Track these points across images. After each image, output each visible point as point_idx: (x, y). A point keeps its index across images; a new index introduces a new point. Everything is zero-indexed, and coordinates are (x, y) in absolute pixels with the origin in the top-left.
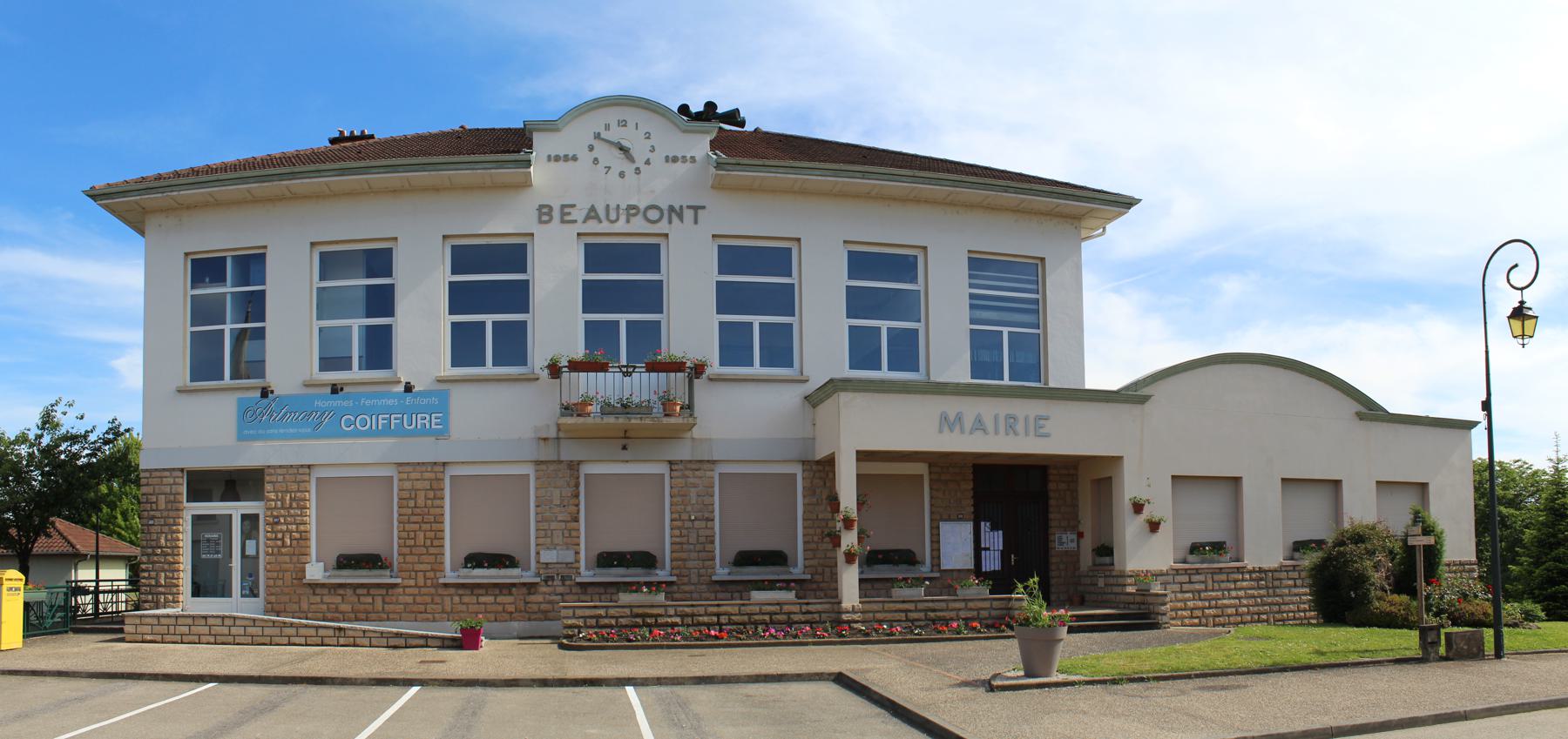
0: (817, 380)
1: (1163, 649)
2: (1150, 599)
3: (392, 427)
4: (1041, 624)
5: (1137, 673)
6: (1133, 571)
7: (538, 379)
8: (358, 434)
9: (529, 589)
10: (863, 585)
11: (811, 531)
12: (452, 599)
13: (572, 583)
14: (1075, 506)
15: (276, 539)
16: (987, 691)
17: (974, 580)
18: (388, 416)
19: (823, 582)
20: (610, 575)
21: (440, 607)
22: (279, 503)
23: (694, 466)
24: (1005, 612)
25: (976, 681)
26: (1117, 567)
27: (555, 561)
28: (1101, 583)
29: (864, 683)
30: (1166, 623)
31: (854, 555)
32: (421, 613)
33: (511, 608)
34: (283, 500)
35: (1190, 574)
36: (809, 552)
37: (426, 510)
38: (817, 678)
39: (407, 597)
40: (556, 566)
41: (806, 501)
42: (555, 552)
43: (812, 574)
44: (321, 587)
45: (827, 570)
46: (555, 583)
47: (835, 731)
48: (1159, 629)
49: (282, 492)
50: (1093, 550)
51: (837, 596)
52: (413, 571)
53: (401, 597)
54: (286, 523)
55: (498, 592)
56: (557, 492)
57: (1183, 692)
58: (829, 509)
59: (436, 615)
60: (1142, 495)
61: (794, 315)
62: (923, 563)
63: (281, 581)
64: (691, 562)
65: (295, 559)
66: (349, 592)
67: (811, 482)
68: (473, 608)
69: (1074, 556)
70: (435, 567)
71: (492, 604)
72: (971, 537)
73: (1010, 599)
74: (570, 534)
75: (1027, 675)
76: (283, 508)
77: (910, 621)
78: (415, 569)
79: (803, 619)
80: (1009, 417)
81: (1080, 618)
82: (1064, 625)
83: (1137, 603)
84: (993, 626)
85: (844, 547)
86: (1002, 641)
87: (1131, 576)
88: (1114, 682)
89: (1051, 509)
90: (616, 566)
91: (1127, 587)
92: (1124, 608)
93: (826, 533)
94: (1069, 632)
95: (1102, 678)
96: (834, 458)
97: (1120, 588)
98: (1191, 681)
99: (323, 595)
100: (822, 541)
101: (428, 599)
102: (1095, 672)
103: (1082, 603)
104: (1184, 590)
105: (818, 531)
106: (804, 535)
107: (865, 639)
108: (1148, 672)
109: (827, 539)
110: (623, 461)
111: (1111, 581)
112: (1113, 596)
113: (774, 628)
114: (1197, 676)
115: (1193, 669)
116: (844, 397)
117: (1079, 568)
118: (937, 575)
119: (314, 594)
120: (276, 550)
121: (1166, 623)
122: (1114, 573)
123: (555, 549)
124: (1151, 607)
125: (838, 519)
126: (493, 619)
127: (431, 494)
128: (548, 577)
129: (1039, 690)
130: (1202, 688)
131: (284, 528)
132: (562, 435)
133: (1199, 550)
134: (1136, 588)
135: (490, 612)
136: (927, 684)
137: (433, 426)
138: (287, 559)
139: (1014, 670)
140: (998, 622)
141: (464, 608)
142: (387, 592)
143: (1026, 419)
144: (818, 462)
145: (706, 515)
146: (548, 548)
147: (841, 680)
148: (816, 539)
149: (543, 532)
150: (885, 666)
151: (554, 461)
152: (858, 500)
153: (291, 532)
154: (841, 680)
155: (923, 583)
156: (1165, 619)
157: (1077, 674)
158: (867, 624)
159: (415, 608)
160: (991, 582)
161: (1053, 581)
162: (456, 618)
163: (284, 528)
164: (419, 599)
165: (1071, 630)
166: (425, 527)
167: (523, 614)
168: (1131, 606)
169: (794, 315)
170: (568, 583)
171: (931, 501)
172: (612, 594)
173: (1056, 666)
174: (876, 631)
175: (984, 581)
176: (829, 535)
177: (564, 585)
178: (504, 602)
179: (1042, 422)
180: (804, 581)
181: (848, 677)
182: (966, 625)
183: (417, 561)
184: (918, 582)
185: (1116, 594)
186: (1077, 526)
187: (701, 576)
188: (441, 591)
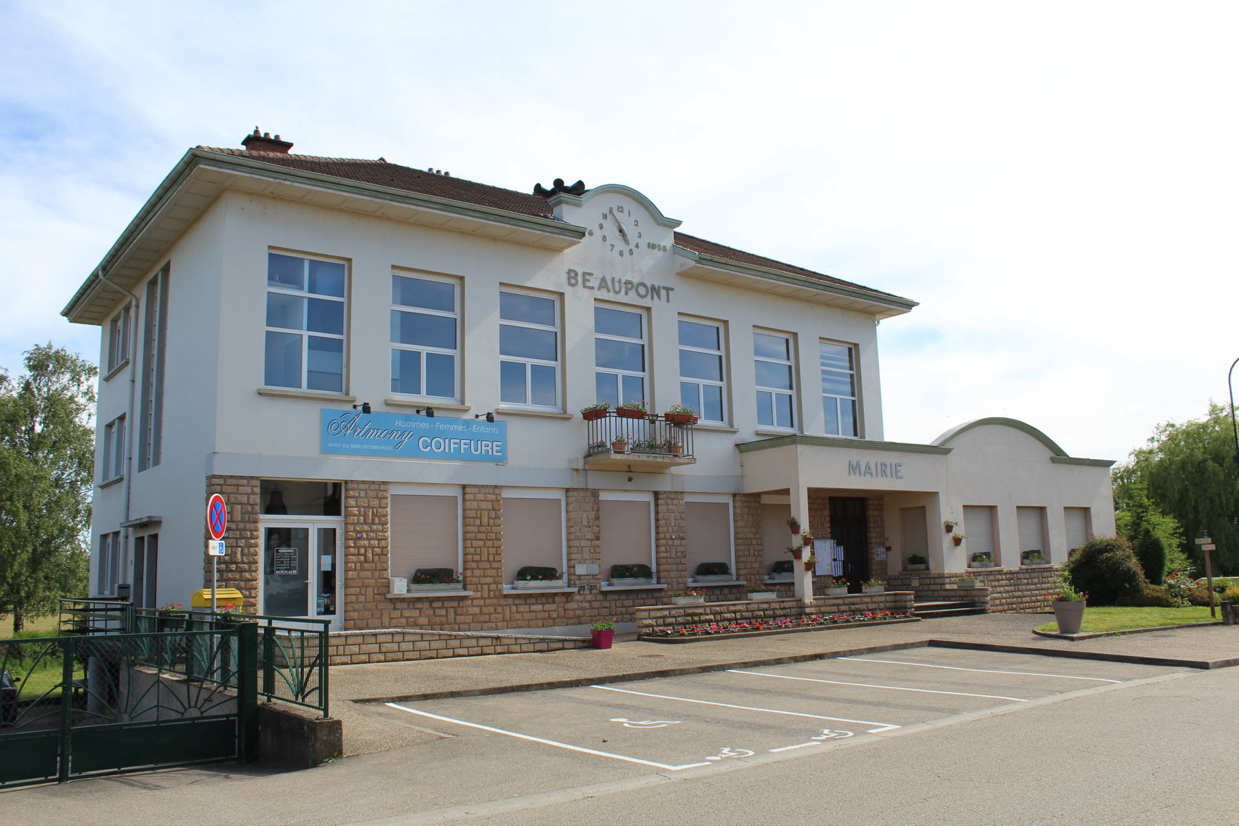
3: (462, 452)
7: (570, 419)
8: (432, 456)
9: (567, 598)
12: (510, 608)
13: (597, 591)
15: (359, 554)
18: (469, 441)
20: (624, 584)
21: (501, 616)
22: (362, 518)
23: (673, 497)
26: (934, 570)
27: (585, 573)
32: (486, 622)
33: (554, 615)
34: (365, 516)
37: (489, 528)
39: (475, 608)
40: (586, 577)
42: (585, 565)
44: (401, 602)
46: (585, 593)
49: (363, 507)
52: (479, 584)
53: (470, 609)
54: (367, 539)
55: (544, 601)
56: (585, 515)
59: (499, 624)
63: (363, 597)
64: (673, 573)
65: (377, 573)
66: (426, 605)
68: (527, 616)
70: (498, 579)
71: (540, 611)
74: (595, 551)
76: (365, 523)
78: (482, 582)
90: (627, 577)
99: (402, 609)
101: (492, 609)
110: (624, 490)
119: (395, 609)
120: (358, 565)
122: (928, 576)
123: (585, 563)
126: (541, 625)
127: (493, 514)
128: (581, 587)
131: (366, 542)
132: (587, 467)
135: (539, 619)
137: (495, 453)
138: (369, 574)
141: (519, 616)
142: (459, 604)
144: (745, 495)
145: (681, 535)
146: (580, 563)
149: (576, 549)
151: (583, 489)
153: (373, 548)
159: (482, 618)
162: (514, 625)
163: (366, 542)
164: (485, 610)
166: (489, 543)
167: (564, 620)
170: (594, 591)
172: (624, 600)
177: (591, 593)
178: (550, 609)
183: (482, 574)
187: (680, 583)
188: (502, 602)
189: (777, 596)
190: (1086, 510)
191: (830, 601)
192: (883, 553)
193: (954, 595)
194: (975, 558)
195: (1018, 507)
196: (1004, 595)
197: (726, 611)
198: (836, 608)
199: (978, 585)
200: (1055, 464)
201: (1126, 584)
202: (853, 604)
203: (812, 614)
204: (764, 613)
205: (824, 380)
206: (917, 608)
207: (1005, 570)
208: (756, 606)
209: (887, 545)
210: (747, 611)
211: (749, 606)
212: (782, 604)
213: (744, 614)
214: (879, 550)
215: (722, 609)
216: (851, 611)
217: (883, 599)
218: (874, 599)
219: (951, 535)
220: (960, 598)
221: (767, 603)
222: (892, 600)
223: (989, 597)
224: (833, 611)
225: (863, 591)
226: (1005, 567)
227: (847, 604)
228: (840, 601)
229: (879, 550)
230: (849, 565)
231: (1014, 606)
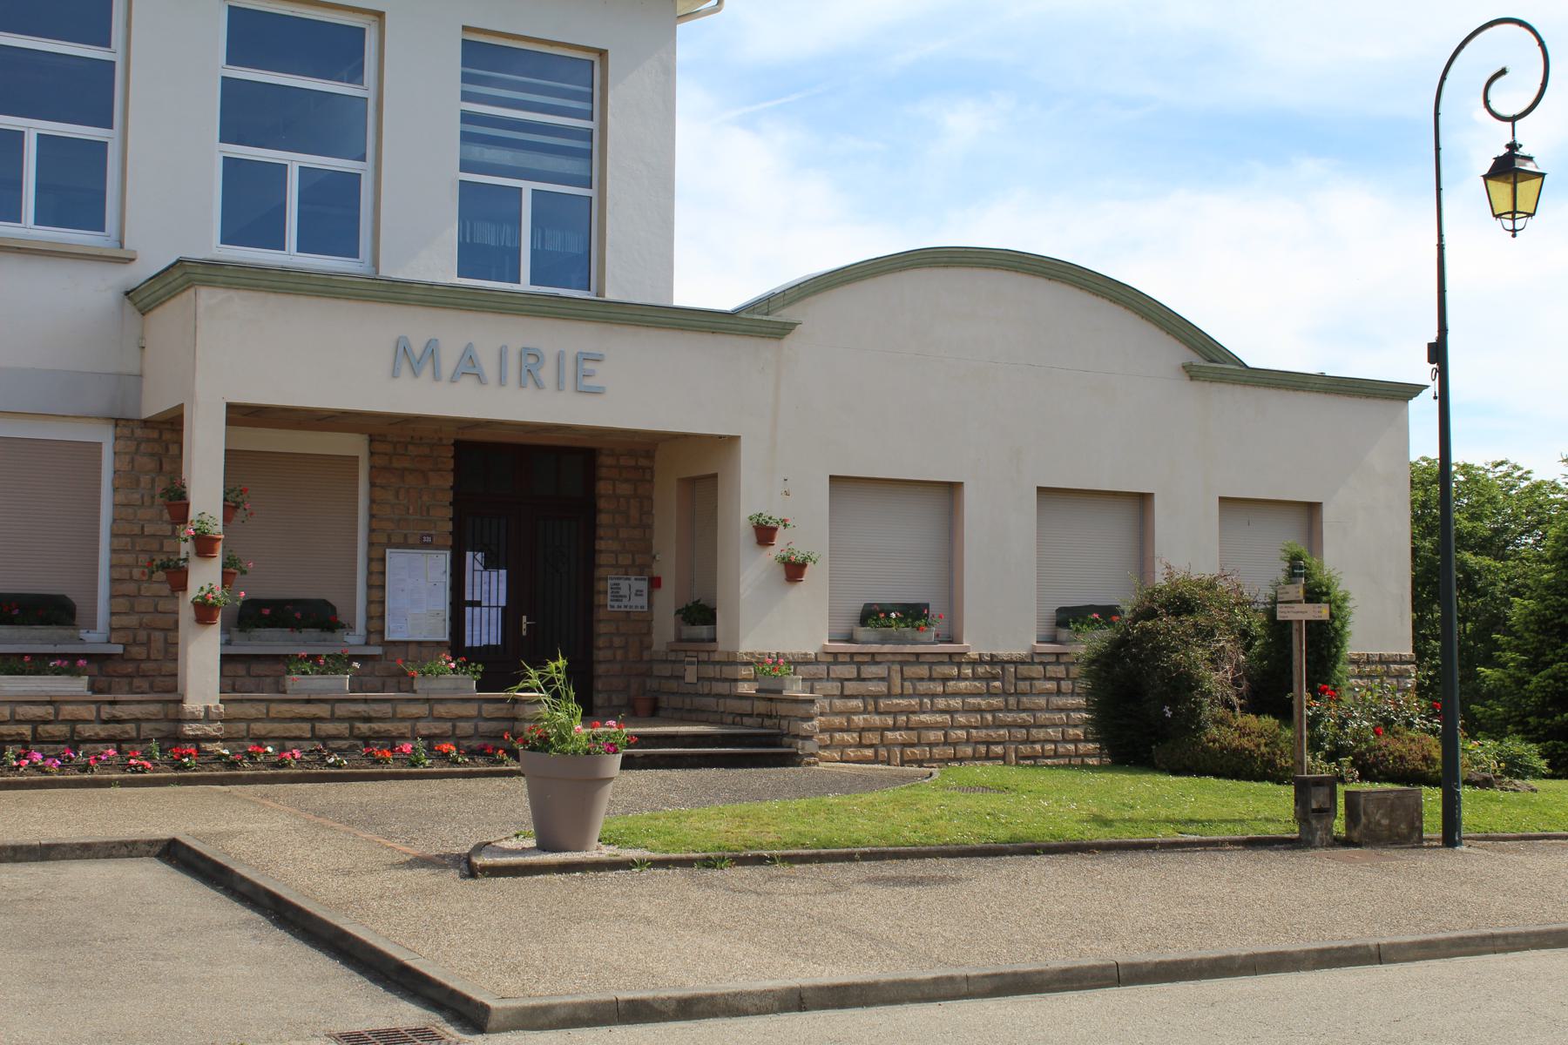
0: (152, 259)
1: (804, 803)
2: (783, 709)
4: (571, 747)
5: (751, 848)
6: (752, 654)
10: (230, 668)
11: (128, 559)
14: (646, 527)
16: (463, 877)
17: (448, 662)
19: (148, 659)
24: (505, 725)
25: (444, 857)
26: (722, 645)
28: (691, 674)
29: (220, 859)
30: (812, 755)
31: (213, 607)
35: (859, 664)
36: (121, 600)
38: (124, 851)
41: (121, 498)
43: (125, 645)
45: (158, 635)
47: (156, 956)
48: (799, 765)
50: (678, 612)
51: (175, 689)
57: (838, 887)
58: (167, 516)
60: (773, 511)
61: (110, 126)
62: (351, 627)
67: (132, 461)
69: (641, 624)
72: (446, 580)
73: (516, 701)
75: (543, 847)
77: (320, 738)
79: (103, 734)
80: (526, 353)
81: (644, 740)
82: (616, 752)
83: (759, 715)
84: (481, 752)
85: (194, 590)
86: (498, 781)
87: (749, 664)
88: (708, 863)
89: (601, 532)
91: (740, 684)
92: (734, 723)
93: (158, 562)
94: (624, 766)
95: (684, 856)
96: (181, 416)
97: (727, 685)
98: (853, 865)
100: (151, 577)
102: (673, 843)
103: (654, 712)
104: (846, 693)
105: (144, 559)
106: (112, 566)
107: (229, 773)
108: (773, 845)
109: (160, 575)
111: (710, 671)
112: (711, 702)
113: (41, 751)
114: (866, 857)
115: (858, 843)
116: (207, 298)
117: (649, 647)
118: (377, 651)
121: (812, 755)
122: (717, 657)
124: (784, 723)
125: (183, 535)
129: (563, 877)
130: (874, 881)
133: (878, 618)
134: (756, 685)
136: (346, 863)
139: (517, 836)
140: (491, 743)
143: (560, 358)
144: (147, 423)
147: (175, 854)
148: (136, 573)
150: (266, 826)
152: (225, 500)
154: (175, 854)
155: (349, 665)
156: (810, 747)
157: (637, 847)
158: (233, 744)
160: (480, 668)
161: (600, 669)
165: (629, 763)
168: (746, 720)
169: (110, 126)
171: (370, 508)
173: (600, 824)
174: (251, 757)
175: (467, 664)
176: (164, 567)
179: (589, 366)
180: (108, 656)
181: (189, 848)
182: (430, 749)
184: (339, 662)
185: (719, 696)
186: (650, 566)
189: (93, 688)
190: (1312, 510)
191: (284, 707)
192: (639, 593)
193: (749, 710)
194: (871, 615)
195: (1040, 489)
196: (962, 719)
198: (347, 725)
200: (1196, 385)
201: (1167, 709)
202: (368, 719)
204: (35, 731)
205: (466, 137)
207: (973, 654)
209: (655, 574)
214: (624, 585)
216: (357, 738)
217: (471, 710)
221: (50, 703)
223: (816, 723)
224: (297, 733)
226: (973, 644)
227: (341, 719)
228: (322, 710)
229: (624, 585)
230: (524, 618)
231: (999, 749)
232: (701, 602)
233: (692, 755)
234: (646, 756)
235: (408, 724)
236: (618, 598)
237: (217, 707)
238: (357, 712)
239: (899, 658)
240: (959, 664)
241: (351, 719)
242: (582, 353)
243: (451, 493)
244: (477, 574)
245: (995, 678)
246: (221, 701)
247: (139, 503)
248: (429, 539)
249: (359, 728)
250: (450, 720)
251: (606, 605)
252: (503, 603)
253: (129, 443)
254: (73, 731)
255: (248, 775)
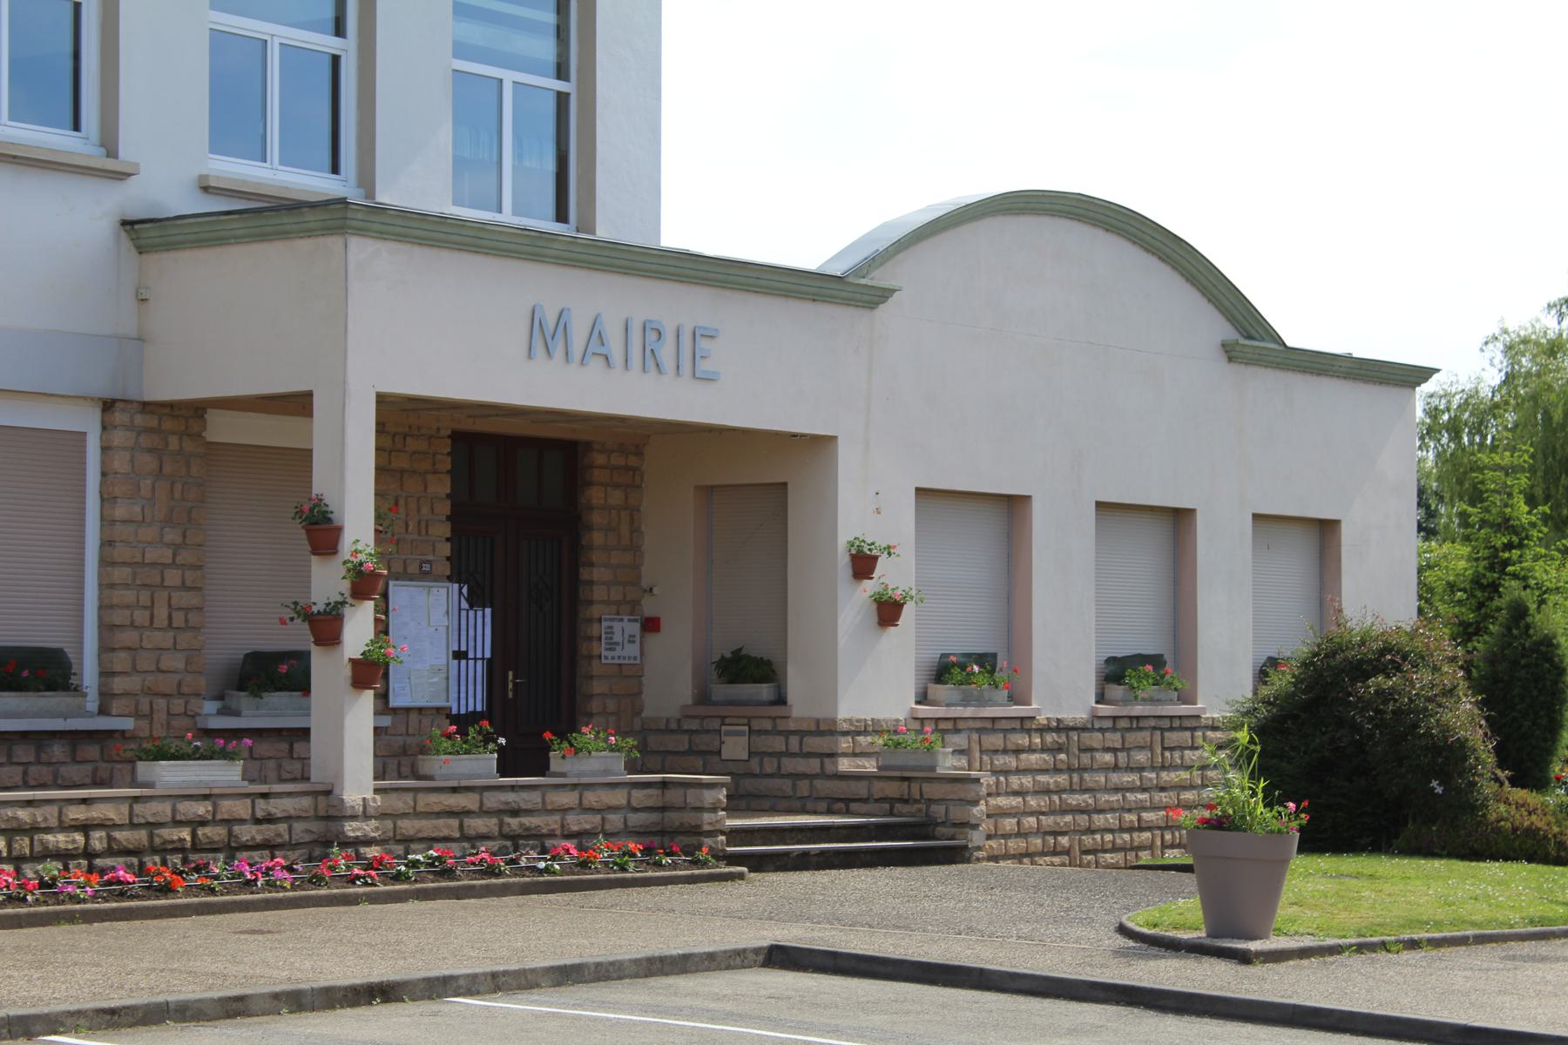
26: (801, 704)
122: (782, 725)
144: (146, 407)
190: (1325, 530)
191: (433, 798)
195: (1100, 506)
196: (1033, 802)
197: (54, 822)
198: (455, 822)
199: (948, 764)
200: (1234, 367)
201: (1434, 784)
202: (515, 813)
203: (369, 842)
204: (194, 835)
206: (737, 835)
208: (163, 810)
210: (133, 826)
211: (138, 808)
212: (261, 803)
213: (117, 834)
215: (39, 814)
217: (619, 797)
218: (591, 798)
219: (869, 587)
220: (887, 806)
221: (206, 797)
222: (650, 803)
223: (982, 807)
224: (445, 832)
225: (555, 764)
226: (1042, 707)
229: (617, 626)
231: (1064, 841)
232: (743, 652)
233: (838, 852)
234: (823, 852)
235: (557, 817)
236: (612, 646)
237: (374, 800)
238: (507, 803)
239: (978, 724)
240: (1029, 731)
241: (498, 813)
242: (700, 327)
243: (448, 503)
244: (464, 613)
245: (1060, 749)
246: (377, 791)
247: (140, 518)
248: (426, 567)
249: (509, 824)
250: (599, 811)
251: (600, 657)
252: (488, 655)
253: (128, 433)
254: (230, 833)
255: (481, 885)
